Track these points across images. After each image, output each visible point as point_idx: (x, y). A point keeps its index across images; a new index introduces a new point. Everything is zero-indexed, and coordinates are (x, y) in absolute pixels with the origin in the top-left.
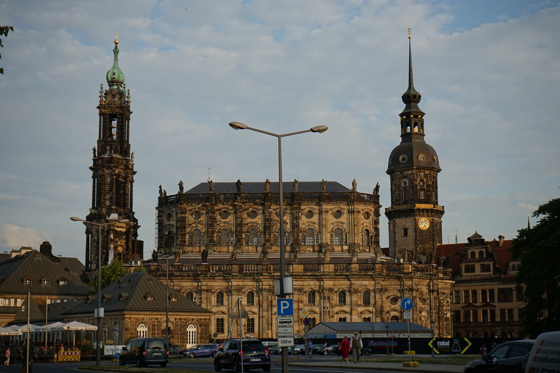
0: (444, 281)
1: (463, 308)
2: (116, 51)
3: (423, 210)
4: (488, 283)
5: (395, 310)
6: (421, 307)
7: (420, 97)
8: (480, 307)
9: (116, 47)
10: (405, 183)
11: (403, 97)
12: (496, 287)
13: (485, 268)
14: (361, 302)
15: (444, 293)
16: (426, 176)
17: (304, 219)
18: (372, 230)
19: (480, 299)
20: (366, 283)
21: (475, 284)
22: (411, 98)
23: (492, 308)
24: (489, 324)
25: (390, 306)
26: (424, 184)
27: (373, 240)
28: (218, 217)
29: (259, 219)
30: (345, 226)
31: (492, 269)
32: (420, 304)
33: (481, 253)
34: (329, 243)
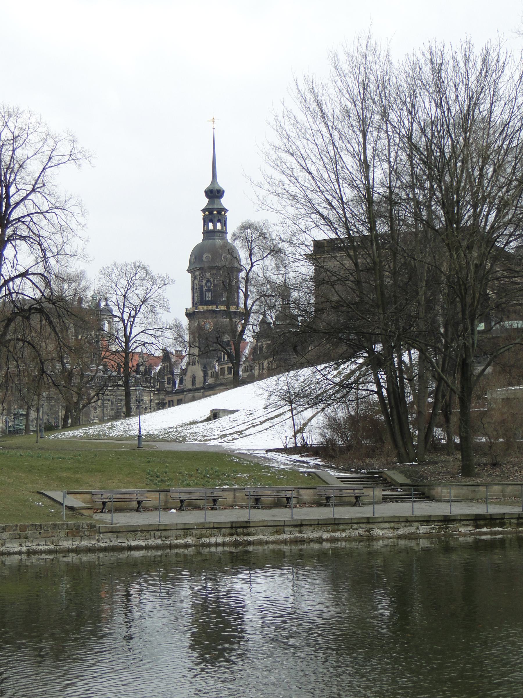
3: (204, 312)
7: (223, 192)
11: (206, 192)
22: (214, 194)
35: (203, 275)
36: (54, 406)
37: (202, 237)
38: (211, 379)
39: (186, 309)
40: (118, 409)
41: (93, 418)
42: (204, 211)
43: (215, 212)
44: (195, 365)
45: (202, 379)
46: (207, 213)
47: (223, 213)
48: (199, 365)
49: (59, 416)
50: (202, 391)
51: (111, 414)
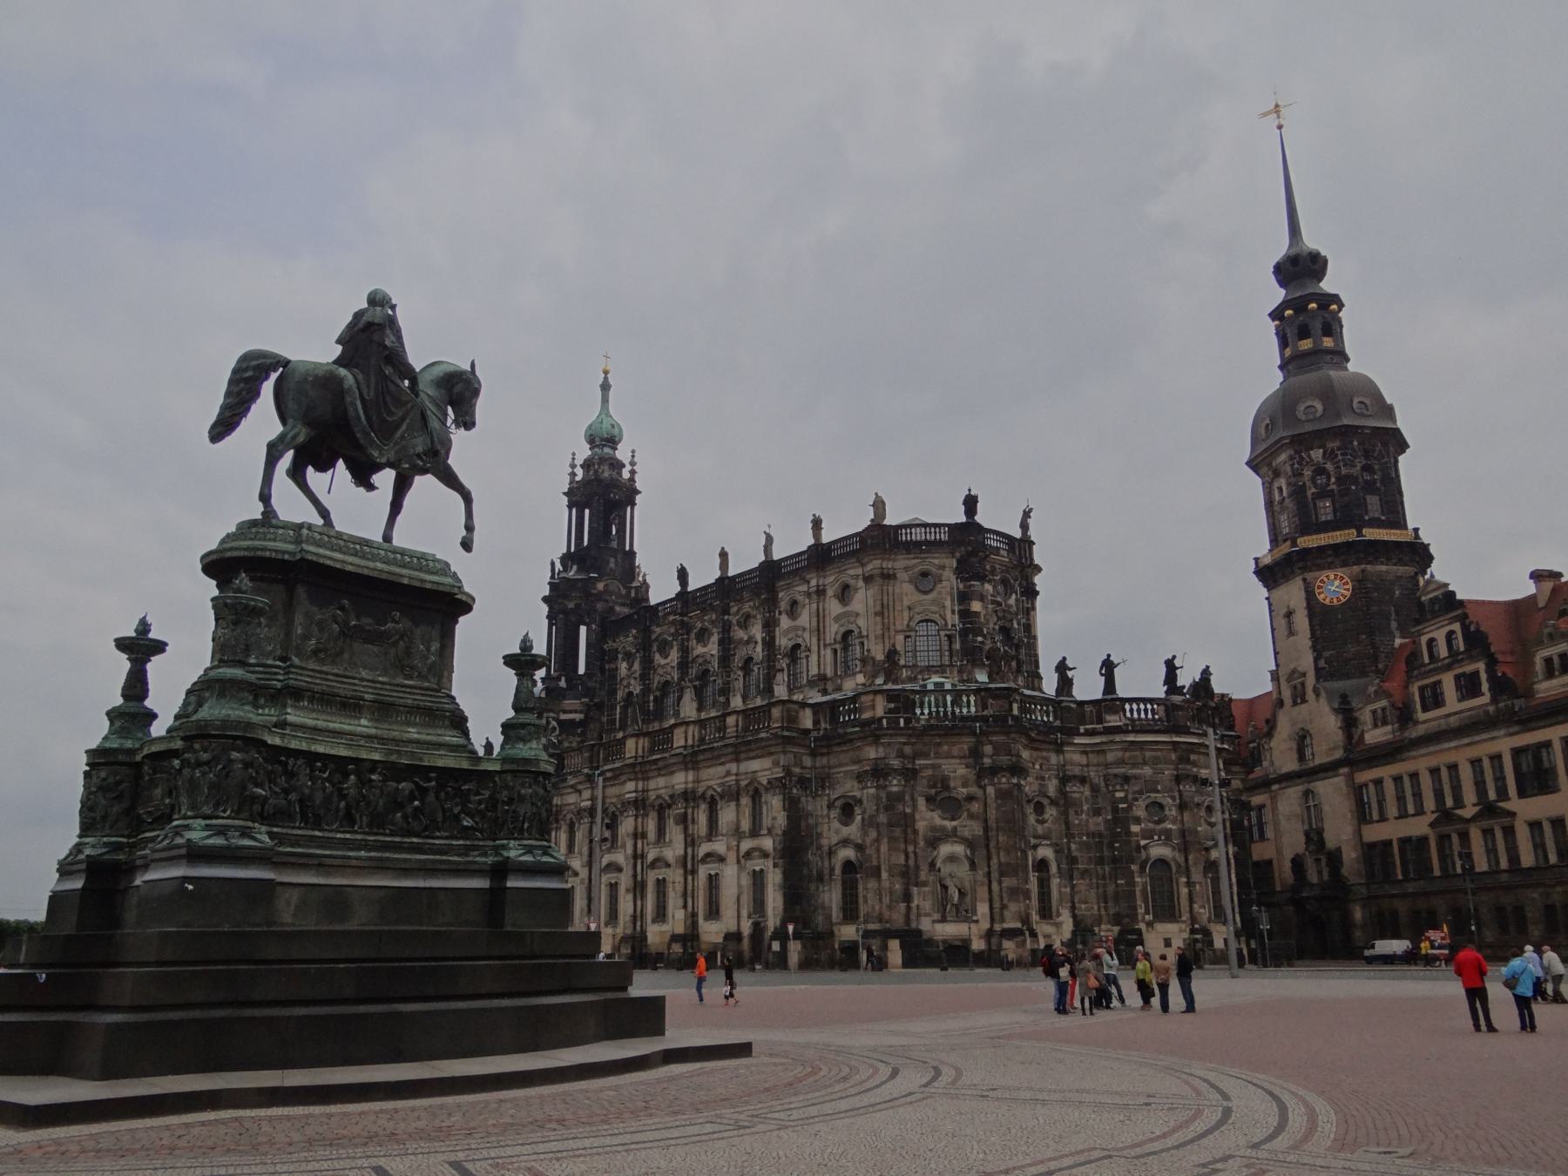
0: (1118, 738)
1: (1432, 825)
2: (605, 387)
3: (1321, 549)
4: (1484, 736)
5: (845, 842)
6: (934, 829)
7: (1325, 261)
8: (1474, 819)
9: (606, 378)
12: (1504, 743)
13: (1469, 686)
14: (746, 825)
15: (1126, 779)
16: (1330, 455)
17: (785, 622)
18: (953, 619)
19: (1470, 796)
20: (755, 765)
21: (1452, 744)
22: (1300, 268)
23: (1506, 821)
24: (1504, 877)
25: (837, 832)
26: (1329, 479)
27: (957, 646)
28: (657, 656)
30: (861, 622)
31: (1485, 687)
33: (1450, 636)
34: (829, 672)
35: (1302, 458)
36: (899, 797)
37: (1279, 377)
38: (1378, 731)
39: (1256, 560)
40: (1115, 810)
41: (1033, 841)
42: (1276, 315)
43: (1314, 305)
44: (1304, 701)
45: (1338, 737)
46: (1289, 312)
47: (1334, 307)
48: (1323, 700)
49: (915, 832)
51: (1092, 828)
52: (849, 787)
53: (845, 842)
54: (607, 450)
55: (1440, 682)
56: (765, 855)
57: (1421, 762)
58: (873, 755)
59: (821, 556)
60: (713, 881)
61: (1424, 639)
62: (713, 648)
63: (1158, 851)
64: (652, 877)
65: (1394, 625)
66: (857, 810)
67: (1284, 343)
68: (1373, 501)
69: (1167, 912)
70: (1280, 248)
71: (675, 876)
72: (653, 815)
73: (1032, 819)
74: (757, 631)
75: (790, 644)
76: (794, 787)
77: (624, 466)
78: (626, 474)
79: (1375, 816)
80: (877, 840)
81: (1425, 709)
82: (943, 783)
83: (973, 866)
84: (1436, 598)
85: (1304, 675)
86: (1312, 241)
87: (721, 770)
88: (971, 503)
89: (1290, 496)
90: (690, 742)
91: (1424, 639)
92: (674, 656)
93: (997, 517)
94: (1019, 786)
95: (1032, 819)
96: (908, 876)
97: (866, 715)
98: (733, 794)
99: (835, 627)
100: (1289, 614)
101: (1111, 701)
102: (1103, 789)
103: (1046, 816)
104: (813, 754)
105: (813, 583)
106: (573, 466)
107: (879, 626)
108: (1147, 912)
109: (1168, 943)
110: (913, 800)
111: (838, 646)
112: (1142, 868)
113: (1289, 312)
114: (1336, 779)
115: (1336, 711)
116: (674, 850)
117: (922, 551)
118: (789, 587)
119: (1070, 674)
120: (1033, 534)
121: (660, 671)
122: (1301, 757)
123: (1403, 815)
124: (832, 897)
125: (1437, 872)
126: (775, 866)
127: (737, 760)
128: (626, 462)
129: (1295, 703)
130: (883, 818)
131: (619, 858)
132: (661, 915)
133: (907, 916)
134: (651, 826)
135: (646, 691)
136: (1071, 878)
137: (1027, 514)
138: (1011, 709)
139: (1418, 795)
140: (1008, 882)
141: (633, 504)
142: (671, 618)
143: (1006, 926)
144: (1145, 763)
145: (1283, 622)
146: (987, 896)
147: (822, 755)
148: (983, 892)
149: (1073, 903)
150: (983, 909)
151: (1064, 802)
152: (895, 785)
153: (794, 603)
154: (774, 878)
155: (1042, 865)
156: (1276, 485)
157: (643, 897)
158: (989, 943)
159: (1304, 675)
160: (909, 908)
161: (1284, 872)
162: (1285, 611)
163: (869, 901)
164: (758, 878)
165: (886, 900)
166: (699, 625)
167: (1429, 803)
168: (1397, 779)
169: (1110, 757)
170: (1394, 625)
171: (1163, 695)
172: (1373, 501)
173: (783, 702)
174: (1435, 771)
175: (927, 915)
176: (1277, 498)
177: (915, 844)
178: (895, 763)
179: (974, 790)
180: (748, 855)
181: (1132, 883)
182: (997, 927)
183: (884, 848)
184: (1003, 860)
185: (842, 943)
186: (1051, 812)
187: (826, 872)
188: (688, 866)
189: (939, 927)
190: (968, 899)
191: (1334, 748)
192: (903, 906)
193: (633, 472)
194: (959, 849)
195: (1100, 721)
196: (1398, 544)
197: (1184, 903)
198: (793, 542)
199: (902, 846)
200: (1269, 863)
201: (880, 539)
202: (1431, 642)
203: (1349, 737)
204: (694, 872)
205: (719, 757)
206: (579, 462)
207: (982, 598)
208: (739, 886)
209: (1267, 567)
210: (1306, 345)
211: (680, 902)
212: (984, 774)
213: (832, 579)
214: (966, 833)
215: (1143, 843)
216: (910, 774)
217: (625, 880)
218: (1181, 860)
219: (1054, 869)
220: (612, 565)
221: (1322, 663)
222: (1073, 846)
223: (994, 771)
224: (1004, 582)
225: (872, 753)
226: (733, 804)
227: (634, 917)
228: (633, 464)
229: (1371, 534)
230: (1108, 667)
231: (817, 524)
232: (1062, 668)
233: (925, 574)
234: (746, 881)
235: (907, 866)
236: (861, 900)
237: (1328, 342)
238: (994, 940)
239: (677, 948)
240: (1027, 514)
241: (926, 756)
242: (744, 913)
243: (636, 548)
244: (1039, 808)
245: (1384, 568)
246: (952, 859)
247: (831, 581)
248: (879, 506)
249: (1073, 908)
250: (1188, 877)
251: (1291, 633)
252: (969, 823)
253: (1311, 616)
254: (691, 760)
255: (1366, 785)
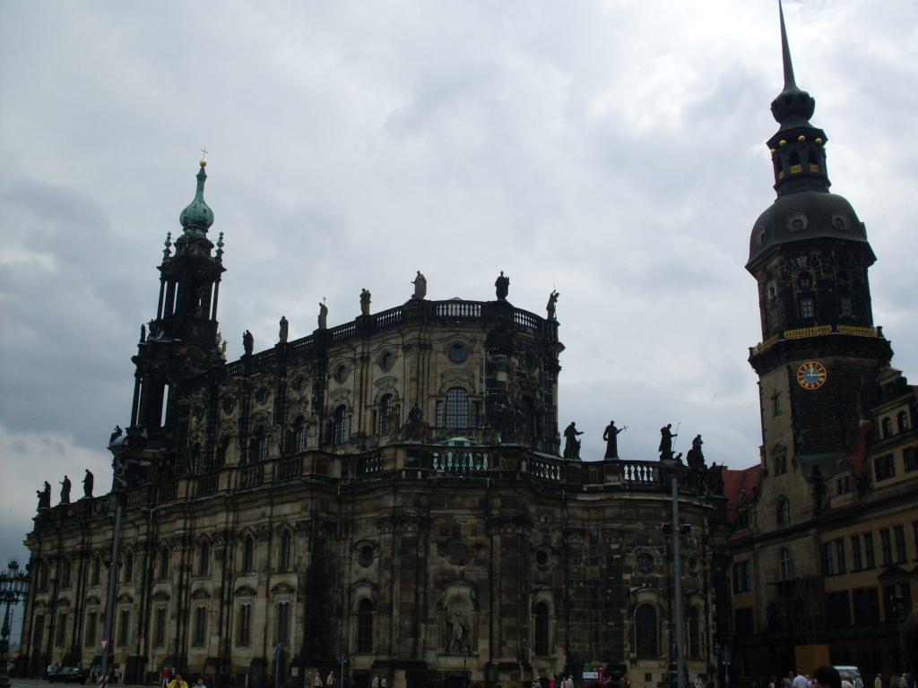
1: (880, 577)
2: (202, 177)
3: (803, 340)
5: (363, 582)
6: (443, 572)
9: (202, 170)
10: (772, 289)
14: (275, 563)
15: (621, 533)
18: (481, 388)
20: (286, 509)
21: (900, 508)
22: (793, 107)
25: (357, 573)
27: (483, 411)
28: (222, 412)
29: (271, 402)
30: (399, 387)
32: (438, 563)
33: (901, 416)
34: (368, 431)
35: (790, 263)
37: (774, 196)
38: (842, 498)
39: (751, 349)
40: (610, 560)
41: (534, 586)
43: (802, 137)
44: (784, 471)
46: (783, 142)
47: (819, 139)
48: (799, 471)
49: (426, 575)
50: (813, 531)
51: (589, 576)
52: (369, 533)
53: (363, 582)
54: (198, 232)
55: (891, 456)
56: (290, 590)
57: (873, 524)
58: (391, 504)
59: (367, 326)
60: (246, 612)
61: (881, 418)
62: (269, 407)
63: (646, 597)
64: (195, 605)
65: (859, 407)
66: (376, 553)
67: (778, 168)
68: (846, 304)
69: (648, 649)
70: (777, 87)
71: (213, 605)
72: (197, 550)
73: (534, 566)
74: (308, 393)
75: (337, 404)
76: (322, 531)
77: (213, 246)
78: (213, 254)
79: (836, 570)
80: (391, 581)
81: (879, 479)
82: (455, 531)
83: (477, 607)
84: (892, 382)
85: (785, 449)
86: (802, 84)
87: (258, 512)
88: (502, 284)
89: (780, 294)
90: (232, 486)
91: (881, 418)
92: (237, 411)
93: (527, 298)
94: (522, 536)
95: (534, 566)
96: (417, 614)
97: (388, 467)
98: (266, 534)
99: (375, 391)
100: (775, 397)
101: (612, 462)
102: (601, 542)
103: (548, 564)
104: (340, 501)
105: (359, 350)
106: (168, 244)
107: (414, 391)
108: (632, 651)
109: (648, 677)
110: (426, 546)
111: (377, 408)
112: (631, 611)
113: (783, 142)
114: (804, 539)
115: (809, 480)
116: (213, 584)
117: (456, 325)
118: (338, 353)
119: (577, 438)
120: (559, 315)
121: (225, 426)
122: (780, 520)
123: (858, 569)
124: (350, 630)
125: (883, 619)
126: (299, 600)
127: (272, 505)
128: (215, 243)
129: (777, 474)
130: (397, 561)
131: (167, 587)
132: (200, 640)
133: (414, 653)
134: (196, 560)
135: (210, 443)
136: (568, 620)
137: (554, 298)
138: (520, 466)
139: (870, 552)
140: (507, 621)
141: (218, 280)
142: (236, 378)
143: (502, 660)
144: (638, 520)
145: (770, 403)
146: (487, 633)
147: (348, 502)
148: (485, 630)
149: (568, 642)
150: (484, 645)
151: (565, 552)
152: (410, 531)
153: (342, 368)
154: (297, 610)
155: (541, 608)
156: (769, 286)
157: (186, 623)
158: (487, 675)
159: (785, 449)
160: (416, 643)
161: (761, 618)
162: (772, 394)
163: (380, 636)
164: (283, 610)
165: (396, 635)
166: (259, 385)
167: (879, 559)
168: (855, 539)
169: (609, 513)
170: (859, 407)
171: (658, 459)
172: (846, 304)
173: (314, 452)
174: (885, 532)
175: (434, 649)
176: (770, 297)
177: (426, 585)
178: (411, 511)
179: (482, 538)
180: (276, 589)
181: (621, 625)
182: (496, 662)
183: (397, 588)
184: (504, 602)
185: (355, 671)
186: (552, 561)
187: (346, 607)
188: (225, 597)
189: (442, 660)
190: (471, 635)
191: (807, 512)
192: (410, 640)
193: (220, 252)
194: (465, 591)
195: (602, 480)
196: (864, 339)
197: (665, 644)
198: (344, 313)
199: (414, 586)
200: (749, 610)
201: (419, 312)
202: (887, 419)
203: (819, 503)
204: (229, 603)
205: (256, 500)
206: (173, 241)
207: (508, 370)
208: (267, 617)
209: (758, 355)
210: (796, 169)
211: (216, 630)
212: (492, 524)
213: (374, 347)
214: (473, 577)
215: (632, 589)
216: (425, 523)
217: (171, 607)
218: (665, 605)
219: (552, 612)
220: (195, 332)
221: (800, 439)
222: (571, 592)
223: (501, 522)
224: (529, 357)
225: (390, 502)
226: (266, 543)
227: (177, 641)
228: (220, 244)
229: (843, 330)
230: (611, 433)
231: (365, 298)
232: (571, 431)
233: (458, 346)
234: (273, 613)
235: (416, 604)
236: (374, 634)
237: (814, 168)
238: (492, 673)
239: (211, 670)
240: (554, 298)
241: (441, 506)
242: (270, 641)
243: (218, 319)
244: (542, 557)
245: (853, 359)
246: (458, 599)
247: (374, 349)
248: (420, 283)
249: (567, 647)
250: (670, 620)
251: (777, 413)
252: (476, 568)
253: (793, 398)
254: (232, 503)
255: (829, 543)
